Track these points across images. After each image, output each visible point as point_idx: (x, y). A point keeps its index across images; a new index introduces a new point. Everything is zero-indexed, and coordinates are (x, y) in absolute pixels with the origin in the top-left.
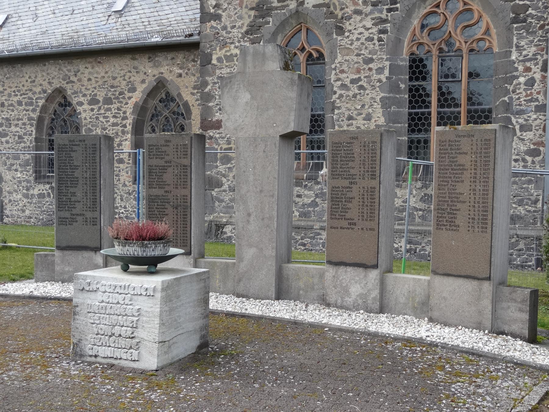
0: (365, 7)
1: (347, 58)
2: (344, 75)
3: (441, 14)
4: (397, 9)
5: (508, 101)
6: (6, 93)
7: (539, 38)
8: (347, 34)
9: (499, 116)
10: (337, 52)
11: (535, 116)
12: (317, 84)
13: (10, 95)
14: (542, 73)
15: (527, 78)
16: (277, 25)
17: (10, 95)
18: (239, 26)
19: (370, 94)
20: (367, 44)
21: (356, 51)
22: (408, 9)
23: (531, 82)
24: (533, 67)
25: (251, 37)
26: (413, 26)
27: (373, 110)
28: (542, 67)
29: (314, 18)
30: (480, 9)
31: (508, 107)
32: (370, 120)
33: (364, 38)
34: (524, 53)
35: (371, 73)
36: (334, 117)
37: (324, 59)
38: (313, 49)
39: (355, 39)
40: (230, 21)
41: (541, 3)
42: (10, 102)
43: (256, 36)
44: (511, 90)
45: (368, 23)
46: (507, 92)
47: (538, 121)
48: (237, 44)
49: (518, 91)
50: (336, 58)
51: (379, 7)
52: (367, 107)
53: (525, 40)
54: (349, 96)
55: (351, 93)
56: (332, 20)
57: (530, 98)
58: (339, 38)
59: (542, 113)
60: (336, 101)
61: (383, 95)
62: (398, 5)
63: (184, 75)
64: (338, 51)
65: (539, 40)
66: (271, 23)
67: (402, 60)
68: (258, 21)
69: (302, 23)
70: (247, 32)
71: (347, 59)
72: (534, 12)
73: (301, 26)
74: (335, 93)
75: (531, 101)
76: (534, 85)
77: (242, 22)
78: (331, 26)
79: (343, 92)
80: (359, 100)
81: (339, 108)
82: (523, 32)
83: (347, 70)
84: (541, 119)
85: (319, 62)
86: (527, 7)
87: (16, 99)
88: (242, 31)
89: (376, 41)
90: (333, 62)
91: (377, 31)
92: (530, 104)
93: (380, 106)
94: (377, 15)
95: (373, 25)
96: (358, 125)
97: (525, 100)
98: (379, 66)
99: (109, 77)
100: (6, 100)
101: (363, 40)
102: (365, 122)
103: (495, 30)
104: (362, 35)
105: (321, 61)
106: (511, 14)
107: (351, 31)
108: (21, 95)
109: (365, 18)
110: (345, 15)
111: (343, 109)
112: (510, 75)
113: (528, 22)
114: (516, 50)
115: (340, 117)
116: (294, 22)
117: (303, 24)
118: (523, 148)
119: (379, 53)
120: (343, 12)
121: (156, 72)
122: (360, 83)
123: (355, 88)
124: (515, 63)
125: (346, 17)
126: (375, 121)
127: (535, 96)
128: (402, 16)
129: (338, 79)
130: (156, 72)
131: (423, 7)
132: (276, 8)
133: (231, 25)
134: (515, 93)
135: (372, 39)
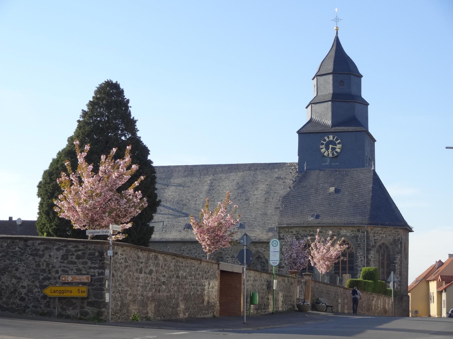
6: (198, 253)
13: (199, 254)
17: (199, 254)
23: (362, 260)
31: (357, 266)
34: (360, 254)
42: (199, 256)
63: (266, 251)
75: (362, 264)
86: (360, 244)
87: (202, 255)
99: (239, 250)
100: (197, 255)
108: (204, 254)
121: (256, 249)
127: (363, 263)
130: (256, 249)
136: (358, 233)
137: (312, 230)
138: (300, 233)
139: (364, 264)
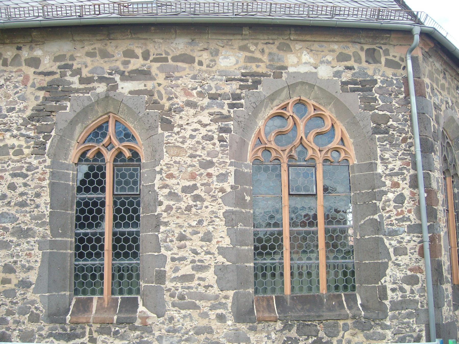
0: (201, 99)
1: (178, 159)
2: (174, 181)
3: (291, 117)
4: (241, 106)
5: (378, 220)
7: (403, 151)
8: (176, 129)
9: (366, 237)
10: (162, 151)
11: (408, 238)
12: (120, 191)
14: (411, 189)
15: (396, 194)
16: (78, 110)
18: (20, 109)
19: (210, 207)
20: (204, 144)
21: (190, 152)
22: (255, 106)
23: (400, 199)
24: (400, 182)
25: (38, 124)
26: (258, 127)
27: (214, 228)
28: (410, 182)
29: (131, 106)
30: (334, 116)
32: (210, 240)
33: (201, 135)
34: (390, 166)
35: (211, 180)
36: (160, 236)
37: (139, 160)
38: (124, 146)
39: (188, 137)
40: (7, 102)
41: (401, 116)
43: (45, 123)
44: (380, 207)
45: (206, 119)
46: (375, 210)
47: (412, 243)
48: (15, 132)
49: (388, 209)
50: (162, 158)
51: (218, 101)
52: (205, 223)
53: (390, 153)
54: (180, 208)
55: (183, 205)
56: (156, 111)
57: (401, 216)
58: (166, 134)
59: (415, 235)
60: (162, 214)
61: (228, 208)
62: (242, 101)
64: (165, 150)
65: (403, 154)
66: (68, 109)
67: (247, 166)
68: (50, 104)
69: (110, 112)
70: (31, 118)
71: (177, 160)
72: (395, 124)
73: (109, 117)
74: (161, 203)
75: (403, 220)
76: (404, 202)
77: (25, 104)
78: (155, 118)
79: (171, 203)
80: (194, 214)
81: (166, 224)
82: (387, 144)
83: (178, 175)
84: (415, 241)
85: (131, 163)
86: (387, 118)
88: (25, 116)
89: (216, 141)
90: (157, 163)
91: (217, 129)
92: (401, 224)
93: (223, 223)
94: (216, 109)
95: (211, 120)
96: (193, 247)
97: (396, 219)
98: (221, 171)
101: (199, 138)
102: (204, 243)
103: (352, 140)
104: (197, 132)
105: (135, 163)
106: (372, 124)
107: (182, 126)
109: (200, 112)
110: (174, 107)
111: (172, 226)
112: (378, 190)
113: (390, 133)
114: (381, 163)
115: (167, 236)
116: (100, 110)
117: (111, 115)
118: (400, 275)
119: (220, 155)
120: (171, 102)
122: (195, 192)
123: (189, 199)
124: (381, 177)
125: (175, 108)
126: (218, 242)
127: (407, 215)
128: (249, 115)
129: (165, 186)
131: (270, 107)
132: (77, 91)
133: (9, 107)
134: (385, 211)
135: (211, 138)
136: (370, 69)
137: (139, 52)
138: (74, 67)
139: (412, 216)
